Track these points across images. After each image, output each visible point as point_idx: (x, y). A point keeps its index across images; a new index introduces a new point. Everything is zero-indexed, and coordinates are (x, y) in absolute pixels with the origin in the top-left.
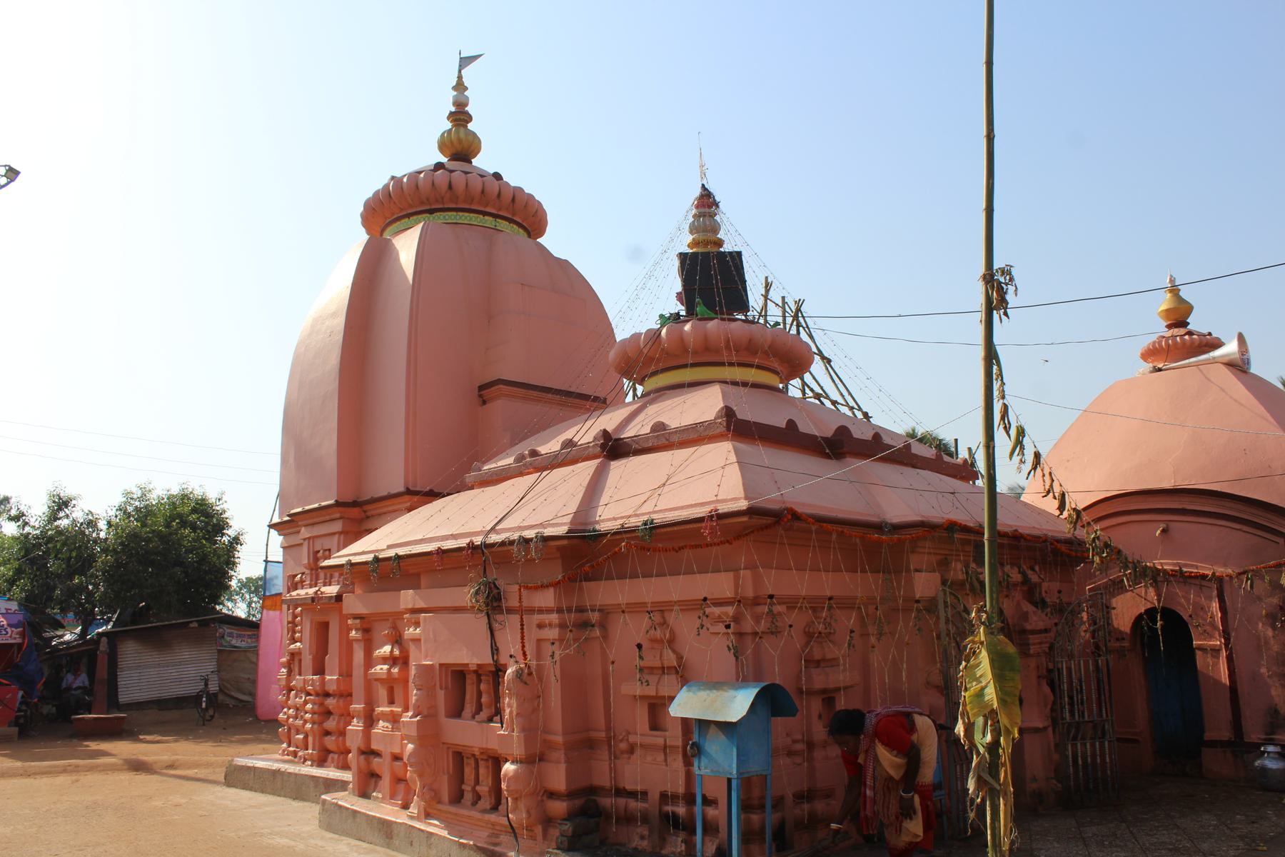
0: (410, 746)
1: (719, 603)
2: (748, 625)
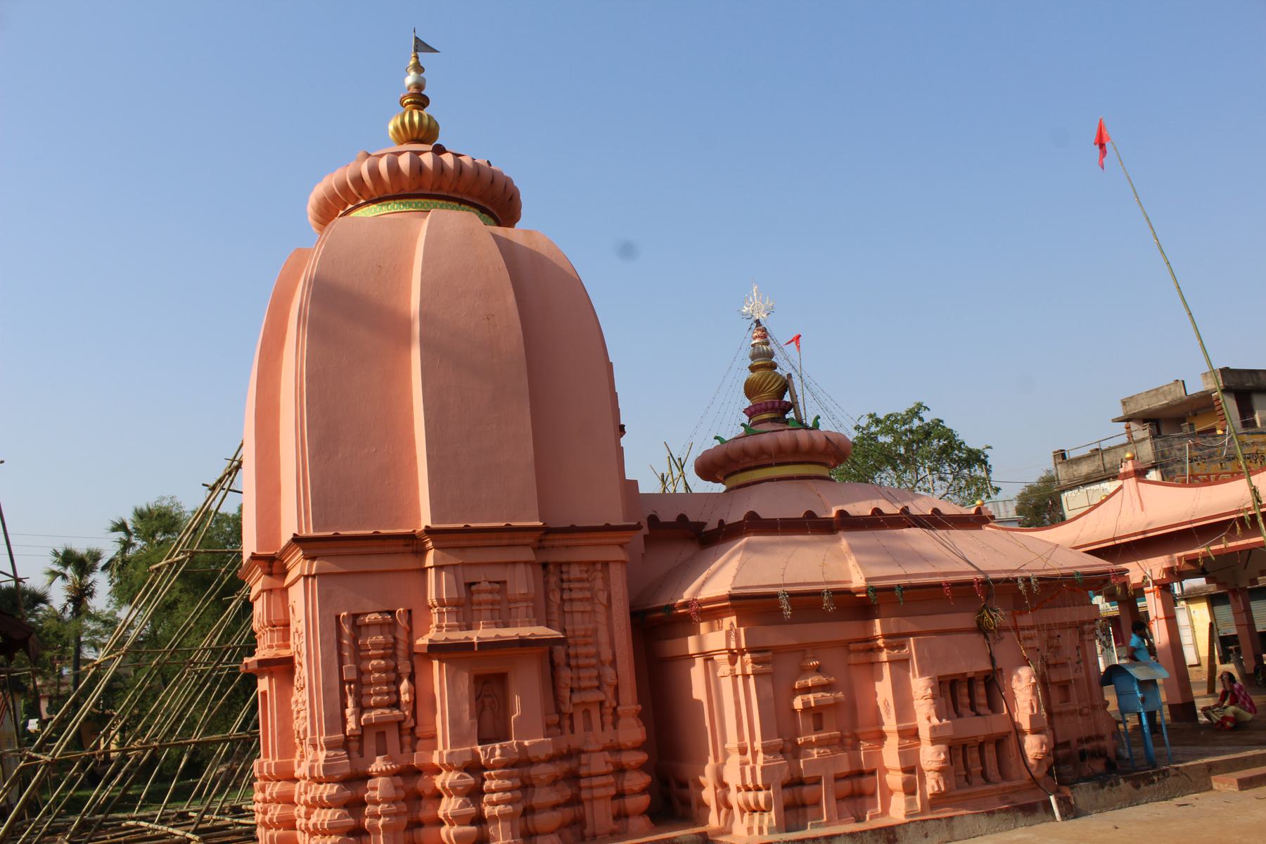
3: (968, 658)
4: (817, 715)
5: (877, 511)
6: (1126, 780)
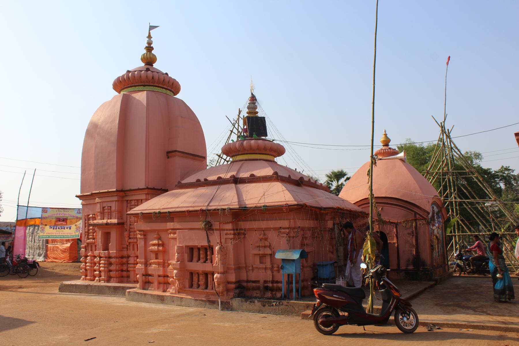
0: (175, 271)
1: (284, 228)
2: (292, 234)
3: (199, 240)
4: (157, 254)
5: (219, 178)
6: (258, 301)
